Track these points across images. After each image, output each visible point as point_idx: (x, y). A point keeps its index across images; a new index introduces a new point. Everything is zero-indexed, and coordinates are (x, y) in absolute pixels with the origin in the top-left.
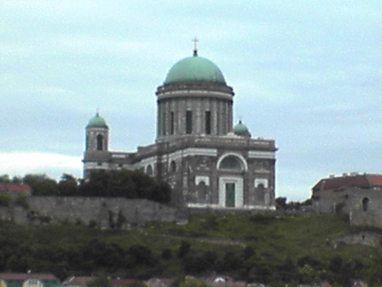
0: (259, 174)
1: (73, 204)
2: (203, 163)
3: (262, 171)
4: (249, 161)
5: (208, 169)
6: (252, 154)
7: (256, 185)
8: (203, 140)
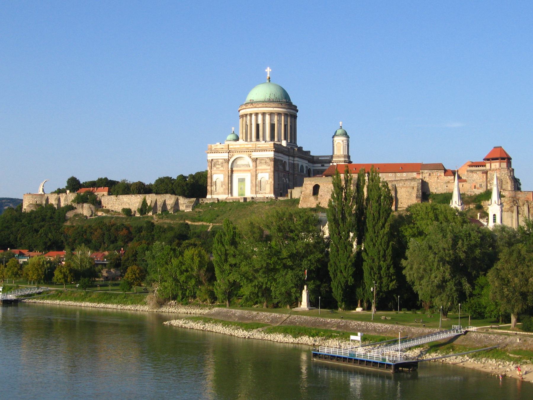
0: (261, 170)
1: (125, 200)
2: (219, 165)
3: (264, 167)
4: (255, 160)
5: (222, 169)
6: (255, 155)
7: (259, 178)
8: (218, 147)
